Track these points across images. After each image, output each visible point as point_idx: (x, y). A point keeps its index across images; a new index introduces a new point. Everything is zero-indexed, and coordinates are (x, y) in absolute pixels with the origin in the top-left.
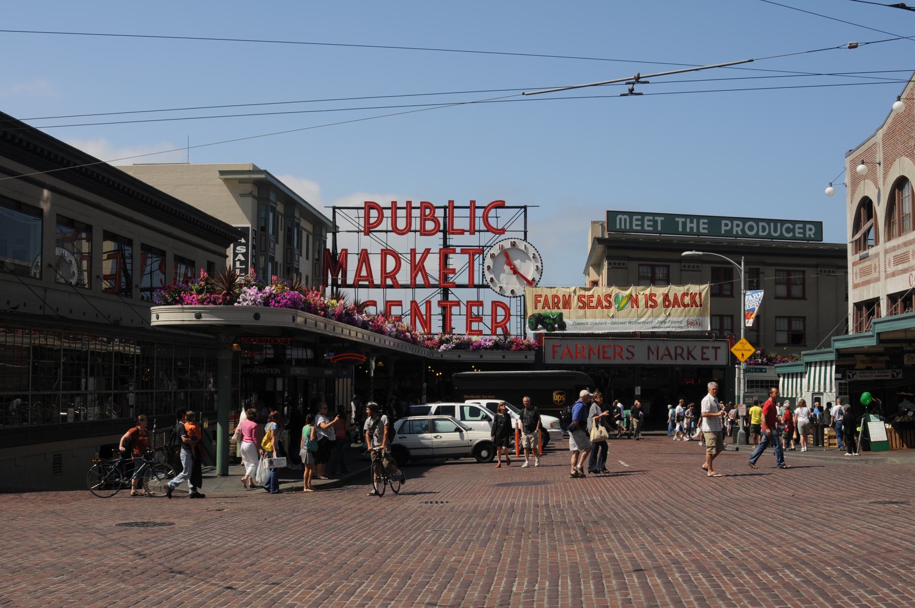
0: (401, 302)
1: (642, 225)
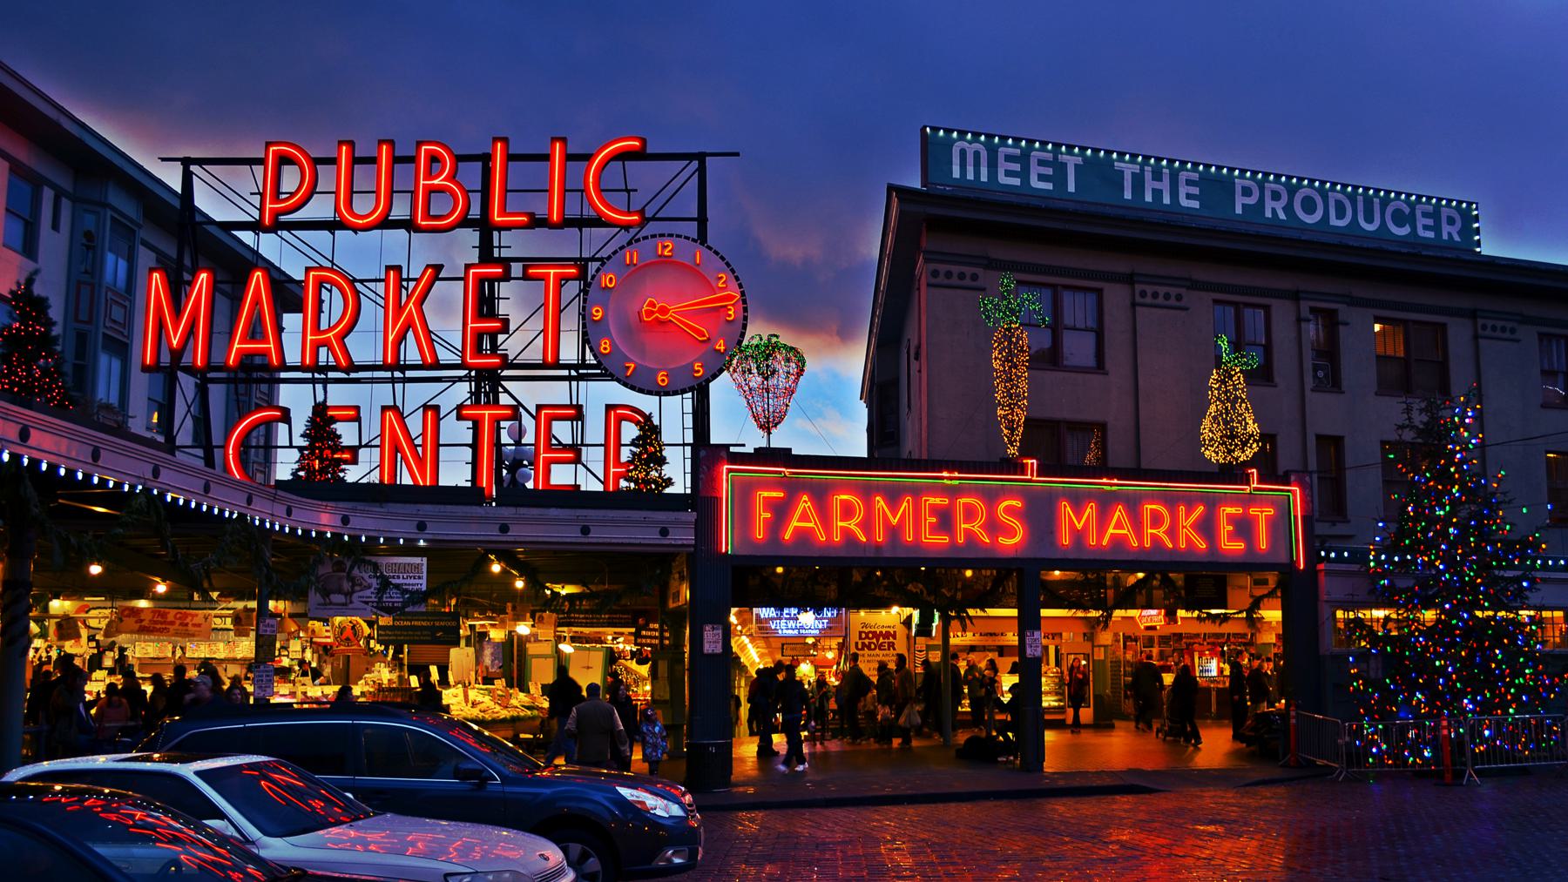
0: (357, 408)
1: (1024, 174)
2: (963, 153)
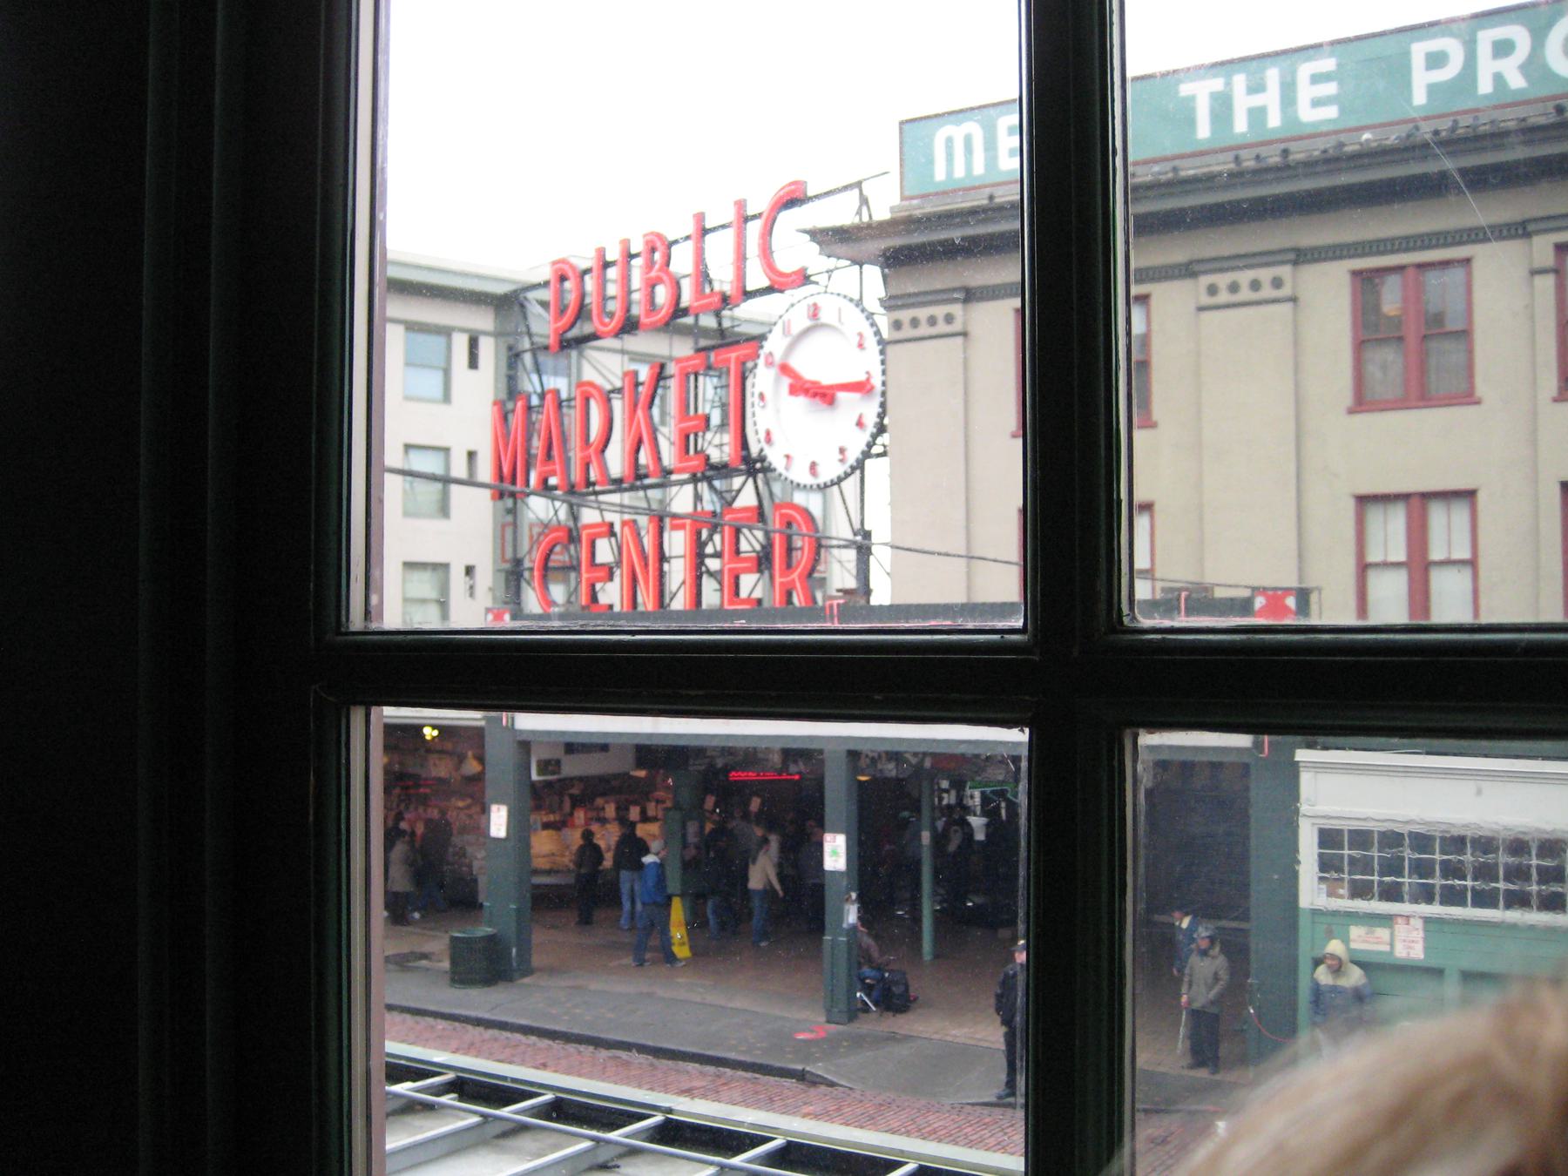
2: (949, 141)
